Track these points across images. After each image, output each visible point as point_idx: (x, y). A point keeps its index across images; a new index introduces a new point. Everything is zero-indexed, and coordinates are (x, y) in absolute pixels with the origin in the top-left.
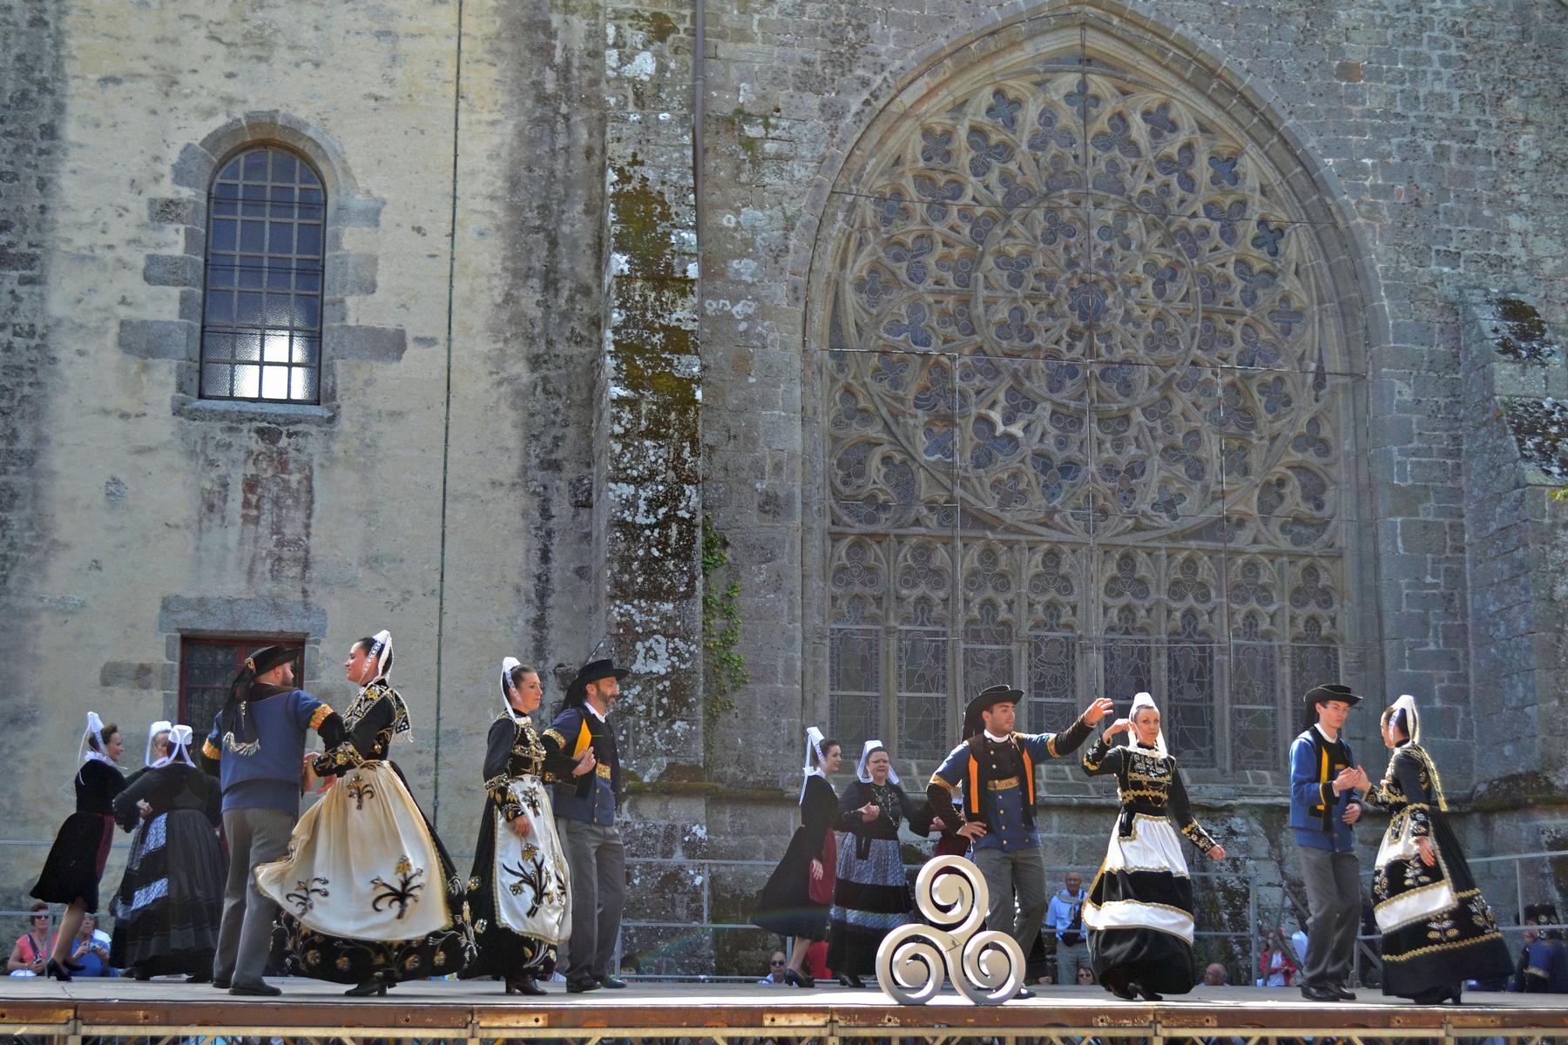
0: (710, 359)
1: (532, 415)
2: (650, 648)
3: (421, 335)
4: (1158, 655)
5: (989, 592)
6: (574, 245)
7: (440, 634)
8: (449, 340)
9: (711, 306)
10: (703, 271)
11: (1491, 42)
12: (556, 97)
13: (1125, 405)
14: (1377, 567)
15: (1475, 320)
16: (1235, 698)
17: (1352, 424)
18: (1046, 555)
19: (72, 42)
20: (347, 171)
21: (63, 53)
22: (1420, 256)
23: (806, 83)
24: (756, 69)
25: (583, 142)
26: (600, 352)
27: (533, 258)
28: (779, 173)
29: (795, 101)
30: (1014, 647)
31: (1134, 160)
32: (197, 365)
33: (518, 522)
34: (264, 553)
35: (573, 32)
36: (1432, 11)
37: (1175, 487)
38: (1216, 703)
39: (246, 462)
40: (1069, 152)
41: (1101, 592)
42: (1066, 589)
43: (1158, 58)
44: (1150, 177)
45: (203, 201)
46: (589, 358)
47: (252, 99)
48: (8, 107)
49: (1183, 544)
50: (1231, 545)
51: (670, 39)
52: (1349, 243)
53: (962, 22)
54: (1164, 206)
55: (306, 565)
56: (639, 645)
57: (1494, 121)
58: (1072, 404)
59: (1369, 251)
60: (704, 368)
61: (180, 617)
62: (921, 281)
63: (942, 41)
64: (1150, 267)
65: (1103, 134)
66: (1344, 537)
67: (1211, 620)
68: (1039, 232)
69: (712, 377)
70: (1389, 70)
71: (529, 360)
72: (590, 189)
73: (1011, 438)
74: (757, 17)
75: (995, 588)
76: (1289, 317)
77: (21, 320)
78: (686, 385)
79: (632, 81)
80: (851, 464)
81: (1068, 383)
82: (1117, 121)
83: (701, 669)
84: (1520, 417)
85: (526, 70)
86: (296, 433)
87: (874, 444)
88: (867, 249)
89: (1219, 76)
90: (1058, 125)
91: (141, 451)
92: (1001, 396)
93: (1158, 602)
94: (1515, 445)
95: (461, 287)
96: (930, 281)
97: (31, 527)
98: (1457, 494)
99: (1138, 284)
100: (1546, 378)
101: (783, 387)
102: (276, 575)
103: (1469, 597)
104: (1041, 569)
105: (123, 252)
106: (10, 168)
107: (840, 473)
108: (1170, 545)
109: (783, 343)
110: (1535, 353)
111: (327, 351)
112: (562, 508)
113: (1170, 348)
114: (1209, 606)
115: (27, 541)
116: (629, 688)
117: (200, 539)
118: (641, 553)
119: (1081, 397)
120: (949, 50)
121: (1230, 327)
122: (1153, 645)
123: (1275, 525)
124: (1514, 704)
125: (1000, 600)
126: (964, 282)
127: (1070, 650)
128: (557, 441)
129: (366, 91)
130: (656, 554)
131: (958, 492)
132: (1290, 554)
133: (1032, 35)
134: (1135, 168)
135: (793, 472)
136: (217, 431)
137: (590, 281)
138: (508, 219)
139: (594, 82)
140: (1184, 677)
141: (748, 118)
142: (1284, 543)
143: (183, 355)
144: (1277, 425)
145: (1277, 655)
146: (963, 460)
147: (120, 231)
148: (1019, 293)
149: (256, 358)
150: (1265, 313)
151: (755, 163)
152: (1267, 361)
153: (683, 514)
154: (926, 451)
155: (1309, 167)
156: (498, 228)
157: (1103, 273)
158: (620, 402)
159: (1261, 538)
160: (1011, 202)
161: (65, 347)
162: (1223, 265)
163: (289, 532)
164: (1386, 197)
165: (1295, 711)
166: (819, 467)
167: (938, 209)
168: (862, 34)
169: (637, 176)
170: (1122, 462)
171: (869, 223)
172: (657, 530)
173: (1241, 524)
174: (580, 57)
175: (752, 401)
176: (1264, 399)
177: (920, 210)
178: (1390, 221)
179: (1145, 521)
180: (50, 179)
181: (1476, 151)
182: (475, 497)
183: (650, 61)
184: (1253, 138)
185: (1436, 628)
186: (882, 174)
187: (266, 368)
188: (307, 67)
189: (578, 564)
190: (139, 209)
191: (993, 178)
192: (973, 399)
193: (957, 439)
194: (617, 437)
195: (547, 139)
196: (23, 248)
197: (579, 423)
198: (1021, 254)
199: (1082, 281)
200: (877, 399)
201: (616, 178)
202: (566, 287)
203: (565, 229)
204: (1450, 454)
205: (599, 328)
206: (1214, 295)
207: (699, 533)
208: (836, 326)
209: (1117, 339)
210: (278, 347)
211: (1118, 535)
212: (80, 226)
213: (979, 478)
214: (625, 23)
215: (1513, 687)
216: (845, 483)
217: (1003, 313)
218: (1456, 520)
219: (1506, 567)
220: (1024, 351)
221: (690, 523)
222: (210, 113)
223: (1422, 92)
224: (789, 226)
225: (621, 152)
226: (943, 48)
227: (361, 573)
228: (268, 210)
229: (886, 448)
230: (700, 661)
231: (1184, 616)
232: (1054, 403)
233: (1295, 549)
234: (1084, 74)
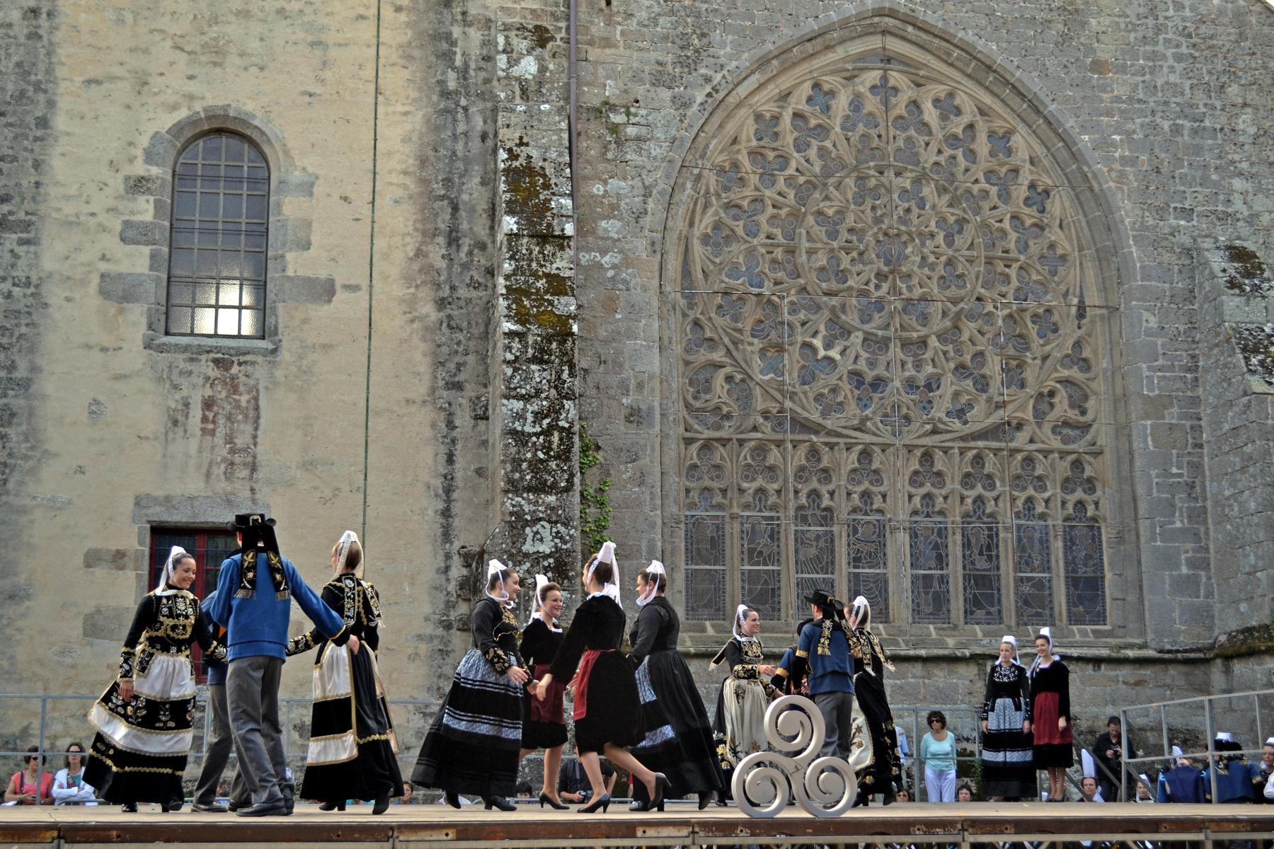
0: (584, 300)
1: (439, 346)
2: (537, 532)
3: (347, 283)
4: (954, 533)
5: (814, 484)
6: (472, 210)
7: (364, 523)
8: (371, 286)
9: (585, 258)
10: (578, 229)
11: (1214, 42)
12: (457, 92)
14: (1132, 461)
15: (1206, 263)
16: (1018, 568)
17: (1108, 346)
18: (860, 454)
19: (60, 51)
20: (287, 153)
21: (54, 60)
22: (1161, 212)
24: (620, 68)
25: (479, 128)
26: (494, 293)
27: (439, 220)
29: (652, 94)
30: (835, 529)
31: (927, 138)
32: (164, 309)
33: (428, 433)
34: (219, 459)
35: (470, 41)
36: (1166, 18)
37: (964, 398)
38: (1002, 571)
39: (204, 385)
40: (874, 132)
41: (907, 483)
42: (877, 481)
43: (945, 57)
44: (940, 152)
45: (169, 178)
46: (485, 300)
47: (208, 95)
48: (9, 103)
49: (972, 444)
50: (1013, 445)
51: (549, 46)
52: (1102, 201)
53: (786, 31)
54: (952, 174)
55: (254, 468)
56: (528, 530)
57: (1218, 104)
58: (880, 333)
59: (1119, 209)
60: (579, 307)
61: (150, 511)
62: (755, 236)
63: (770, 46)
64: (942, 221)
65: (901, 117)
67: (996, 505)
68: (850, 197)
69: (586, 314)
70: (1132, 65)
71: (436, 302)
72: (485, 165)
74: (619, 28)
75: (819, 481)
76: (1055, 260)
77: (20, 273)
78: (564, 320)
79: (518, 79)
81: (876, 316)
82: (912, 107)
83: (579, 548)
84: (1245, 339)
85: (432, 71)
86: (245, 362)
88: (711, 211)
89: (995, 71)
90: (865, 111)
91: (117, 378)
92: (822, 328)
93: (953, 491)
94: (1243, 362)
95: (380, 244)
96: (762, 235)
97: (27, 440)
98: (1195, 401)
99: (932, 235)
100: (1266, 308)
102: (229, 476)
103: (1208, 484)
104: (857, 465)
105: (103, 218)
106: (10, 152)
107: (691, 389)
108: (962, 444)
109: (643, 286)
110: (1256, 288)
111: (271, 296)
112: (463, 420)
114: (995, 494)
115: (23, 451)
116: (520, 563)
117: (166, 449)
118: (529, 455)
121: (1007, 270)
122: (949, 526)
123: (1047, 428)
124: (1247, 569)
125: (824, 490)
126: (790, 236)
127: (881, 531)
128: (459, 366)
129: (302, 89)
130: (541, 455)
132: (1060, 452)
133: (842, 41)
134: (927, 144)
135: (653, 390)
136: (180, 360)
137: (485, 238)
138: (418, 190)
139: (487, 81)
140: (976, 551)
141: (612, 108)
142: (1056, 443)
143: (153, 300)
144: (1048, 348)
145: (1052, 533)
146: (791, 378)
147: (100, 202)
148: (835, 244)
149: (213, 302)
150: (1036, 258)
151: (619, 143)
152: (1038, 299)
153: (563, 424)
154: (761, 372)
155: (1069, 142)
156: (410, 197)
157: (903, 228)
158: (511, 334)
159: (1036, 439)
160: (827, 172)
161: (55, 295)
162: (1001, 221)
163: (240, 441)
164: (1132, 166)
165: (1067, 577)
166: (674, 385)
167: (768, 178)
168: (705, 41)
169: (523, 155)
170: (921, 379)
171: (712, 190)
172: (542, 438)
173: (1019, 427)
174: (476, 61)
175: (619, 333)
176: (1036, 327)
177: (754, 179)
178: (1136, 184)
180: (44, 161)
181: (1204, 128)
182: (392, 412)
183: (533, 63)
184: (1023, 120)
185: (1181, 509)
186: (722, 151)
187: (220, 310)
188: (254, 70)
190: (117, 183)
191: (812, 153)
192: (799, 329)
193: (786, 362)
194: (508, 363)
195: (450, 126)
196: (21, 215)
197: (477, 352)
198: (838, 212)
199: (886, 234)
200: (720, 331)
201: (506, 156)
202: (466, 243)
203: (465, 197)
204: (1189, 370)
205: (493, 276)
206: (994, 245)
207: (576, 439)
208: (686, 272)
209: (915, 281)
210: (230, 294)
211: (919, 437)
212: (68, 198)
213: (805, 393)
214: (513, 34)
216: (695, 398)
217: (821, 260)
218: (1195, 422)
219: (1237, 459)
220: (841, 291)
221: (569, 432)
222: (175, 107)
223: (1160, 82)
224: (647, 194)
225: (509, 136)
226: (771, 52)
227: (299, 474)
228: (222, 184)
229: (728, 370)
230: (578, 542)
231: (974, 502)
233: (1064, 447)
234: (885, 70)
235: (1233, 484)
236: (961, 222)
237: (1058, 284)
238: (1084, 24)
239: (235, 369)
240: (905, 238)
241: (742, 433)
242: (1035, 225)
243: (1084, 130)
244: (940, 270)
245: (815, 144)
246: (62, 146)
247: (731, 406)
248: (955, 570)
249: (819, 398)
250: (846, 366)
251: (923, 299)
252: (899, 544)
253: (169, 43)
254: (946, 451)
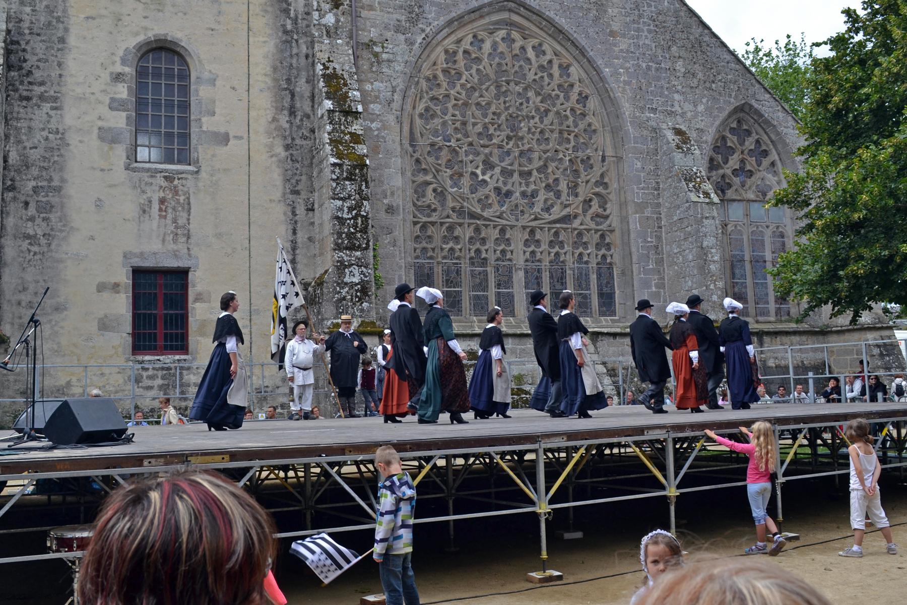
1: (287, 170)
6: (302, 97)
12: (292, 31)
13: (529, 168)
14: (629, 235)
20: (200, 61)
22: (642, 109)
23: (398, 29)
27: (284, 101)
29: (395, 37)
33: (282, 218)
36: (644, 11)
37: (549, 203)
40: (504, 62)
42: (508, 244)
44: (536, 74)
45: (134, 73)
46: (310, 146)
47: (155, 28)
48: (42, 29)
49: (554, 226)
51: (341, 8)
52: (613, 101)
55: (189, 238)
58: (509, 167)
61: (132, 261)
64: (537, 109)
68: (493, 96)
73: (484, 181)
76: (590, 131)
77: (53, 126)
79: (324, 25)
85: (278, 19)
86: (182, 178)
87: (429, 183)
88: (424, 100)
89: (563, 33)
90: (499, 51)
91: (111, 186)
93: (545, 250)
95: (253, 113)
96: (449, 114)
97: (61, 221)
98: (658, 205)
101: (393, 159)
102: (175, 241)
106: (44, 57)
108: (549, 226)
109: (393, 140)
112: (301, 210)
115: (59, 227)
117: (139, 226)
119: (511, 164)
125: (483, 248)
131: (465, 204)
133: (488, 14)
134: (530, 70)
135: (399, 196)
136: (145, 176)
139: (308, 26)
140: (556, 280)
141: (375, 44)
142: (593, 225)
144: (588, 177)
146: (466, 190)
148: (487, 120)
156: (269, 88)
160: (481, 83)
161: (73, 139)
163: (181, 222)
166: (408, 193)
168: (421, 10)
169: (331, 67)
170: (529, 190)
173: (575, 217)
174: (302, 14)
177: (445, 85)
180: (63, 62)
184: (576, 59)
188: (180, 14)
189: (309, 236)
190: (106, 76)
195: (289, 50)
196: (52, 93)
199: (511, 116)
202: (299, 114)
203: (298, 89)
204: (656, 190)
209: (525, 141)
212: (78, 84)
213: (473, 198)
215: (686, 282)
216: (418, 200)
217: (479, 128)
219: (682, 234)
220: (489, 145)
222: (137, 34)
223: (641, 43)
224: (394, 91)
225: (324, 56)
228: (163, 78)
229: (434, 185)
231: (555, 255)
232: (502, 167)
235: (679, 246)
236: (547, 111)
237: (593, 144)
238: (606, 11)
239: (176, 182)
240: (520, 118)
241: (442, 219)
242: (581, 114)
243: (606, 66)
244: (537, 136)
245: (475, 67)
247: (436, 204)
249: (479, 201)
250: (492, 184)
251: (530, 150)
252: (519, 277)
254: (541, 229)
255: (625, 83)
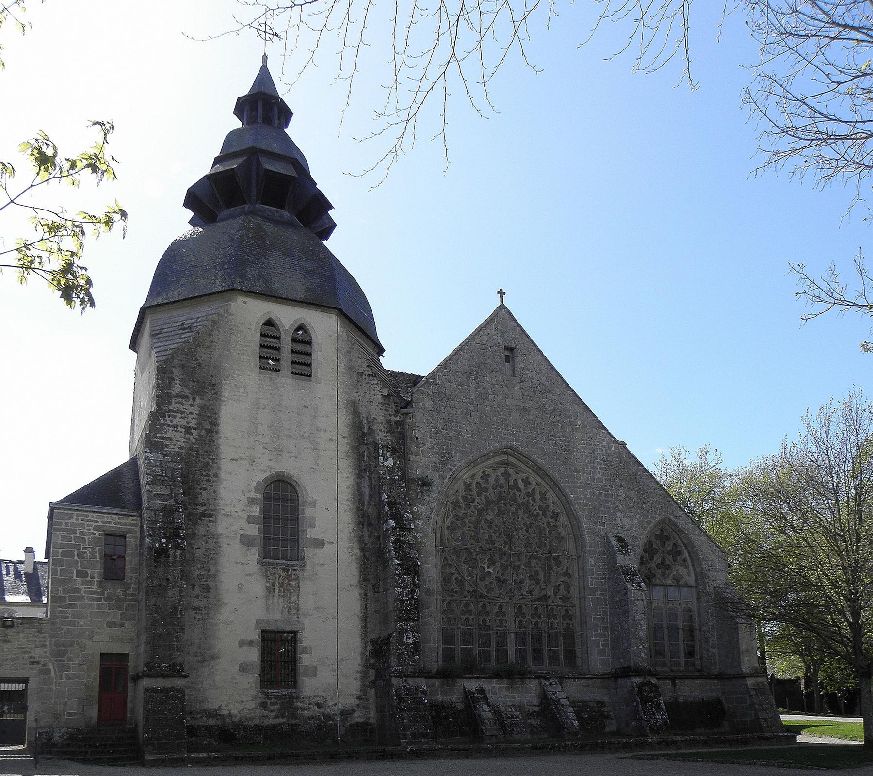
5: (485, 617)
20: (306, 491)
22: (595, 524)
23: (435, 469)
28: (429, 496)
33: (359, 597)
36: (598, 454)
52: (577, 518)
55: (298, 610)
66: (576, 602)
68: (496, 513)
76: (560, 539)
80: (446, 580)
101: (431, 558)
104: (498, 610)
113: (530, 548)
120: (473, 461)
132: (562, 606)
133: (493, 456)
142: (560, 603)
156: (350, 509)
179: (525, 597)
190: (244, 500)
208: (442, 540)
209: (517, 544)
212: (227, 505)
222: (265, 471)
239: (290, 572)
242: (554, 525)
246: (225, 484)
247: (457, 589)
248: (529, 648)
253: (262, 446)
255: (584, 505)
